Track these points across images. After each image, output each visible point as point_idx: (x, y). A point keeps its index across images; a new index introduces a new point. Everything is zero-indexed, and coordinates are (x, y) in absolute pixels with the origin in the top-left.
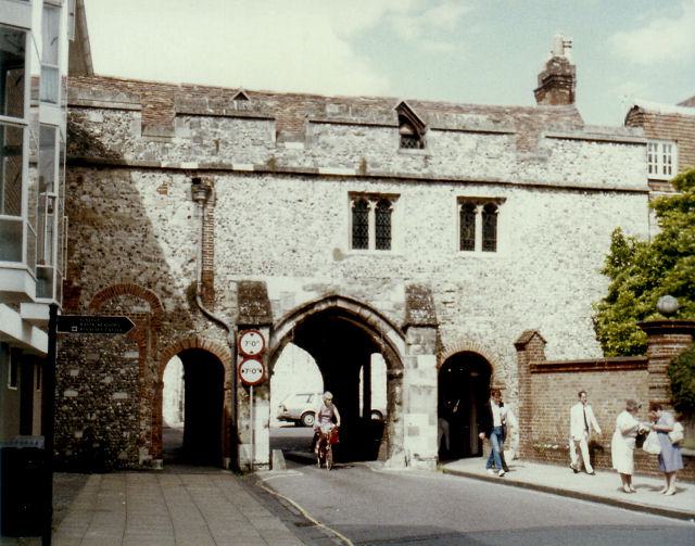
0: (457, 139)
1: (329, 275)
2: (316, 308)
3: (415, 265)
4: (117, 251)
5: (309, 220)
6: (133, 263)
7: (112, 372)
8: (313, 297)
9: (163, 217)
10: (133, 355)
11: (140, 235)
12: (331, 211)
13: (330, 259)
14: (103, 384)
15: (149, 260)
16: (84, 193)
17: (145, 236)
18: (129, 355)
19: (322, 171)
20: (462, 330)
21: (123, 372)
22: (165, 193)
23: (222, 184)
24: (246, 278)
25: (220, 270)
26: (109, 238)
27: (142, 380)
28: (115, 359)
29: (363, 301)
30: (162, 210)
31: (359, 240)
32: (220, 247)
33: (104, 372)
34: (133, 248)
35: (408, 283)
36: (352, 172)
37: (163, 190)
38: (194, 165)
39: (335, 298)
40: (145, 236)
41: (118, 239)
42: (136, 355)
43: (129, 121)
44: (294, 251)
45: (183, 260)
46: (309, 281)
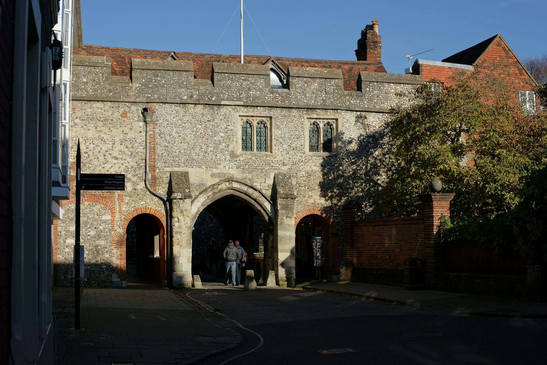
0: (305, 83)
1: (227, 167)
2: (220, 187)
3: (281, 161)
4: (96, 153)
5: (215, 134)
6: (107, 161)
7: (95, 228)
8: (217, 180)
9: (125, 132)
10: (107, 217)
11: (111, 143)
12: (229, 128)
13: (228, 157)
14: (89, 235)
15: (116, 158)
16: (77, 118)
17: (114, 144)
18: (104, 218)
19: (223, 103)
20: (311, 201)
21: (101, 228)
22: (126, 117)
23: (160, 110)
24: (176, 169)
25: (159, 164)
26: (92, 146)
27: (113, 233)
28: (96, 220)
29: (248, 183)
30: (124, 128)
31: (247, 146)
32: (159, 150)
33: (90, 228)
34: (107, 151)
35: (276, 171)
36: (242, 103)
37: (124, 115)
38: (144, 100)
39: (230, 180)
40: (114, 144)
41: (97, 146)
42: (107, 217)
43: (103, 73)
44: (205, 152)
45: (136, 159)
46: (215, 171)
